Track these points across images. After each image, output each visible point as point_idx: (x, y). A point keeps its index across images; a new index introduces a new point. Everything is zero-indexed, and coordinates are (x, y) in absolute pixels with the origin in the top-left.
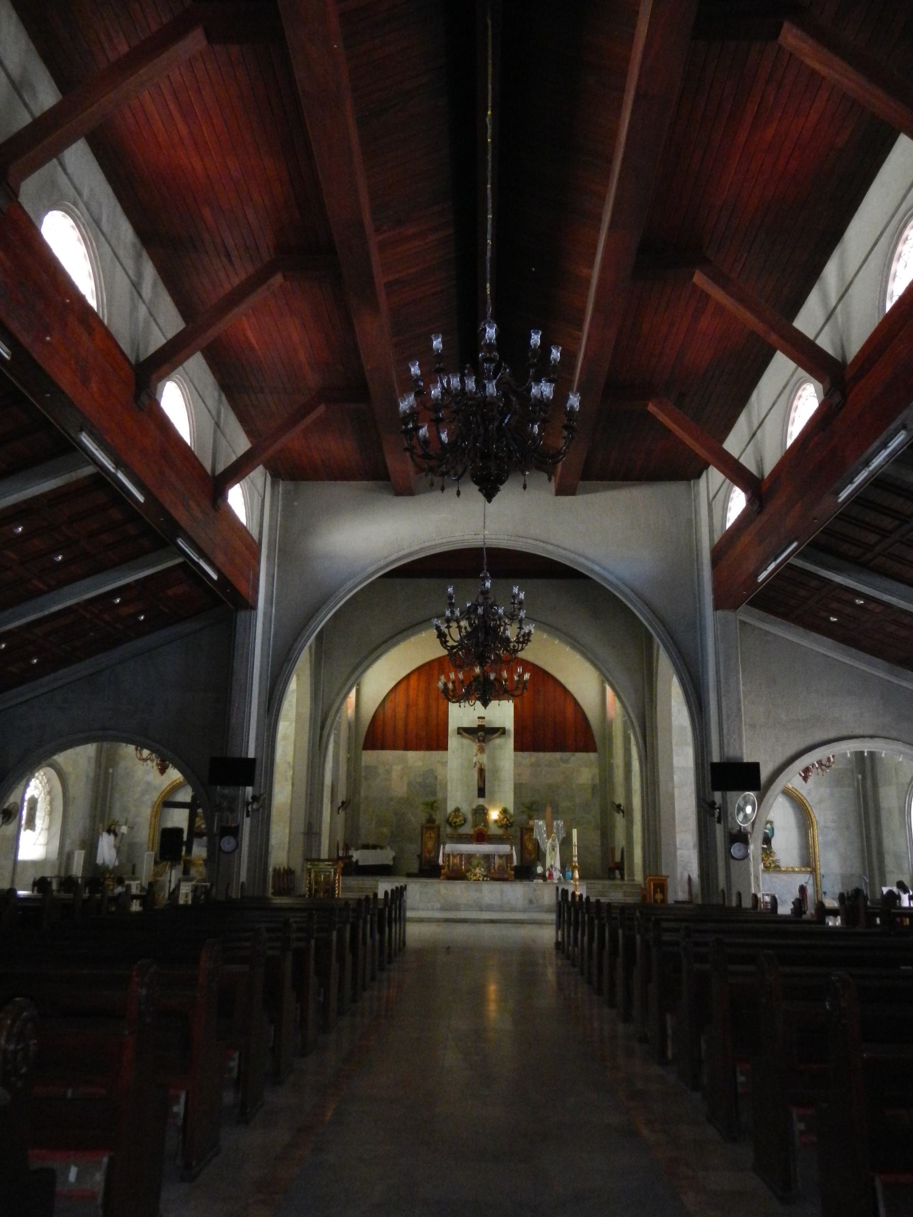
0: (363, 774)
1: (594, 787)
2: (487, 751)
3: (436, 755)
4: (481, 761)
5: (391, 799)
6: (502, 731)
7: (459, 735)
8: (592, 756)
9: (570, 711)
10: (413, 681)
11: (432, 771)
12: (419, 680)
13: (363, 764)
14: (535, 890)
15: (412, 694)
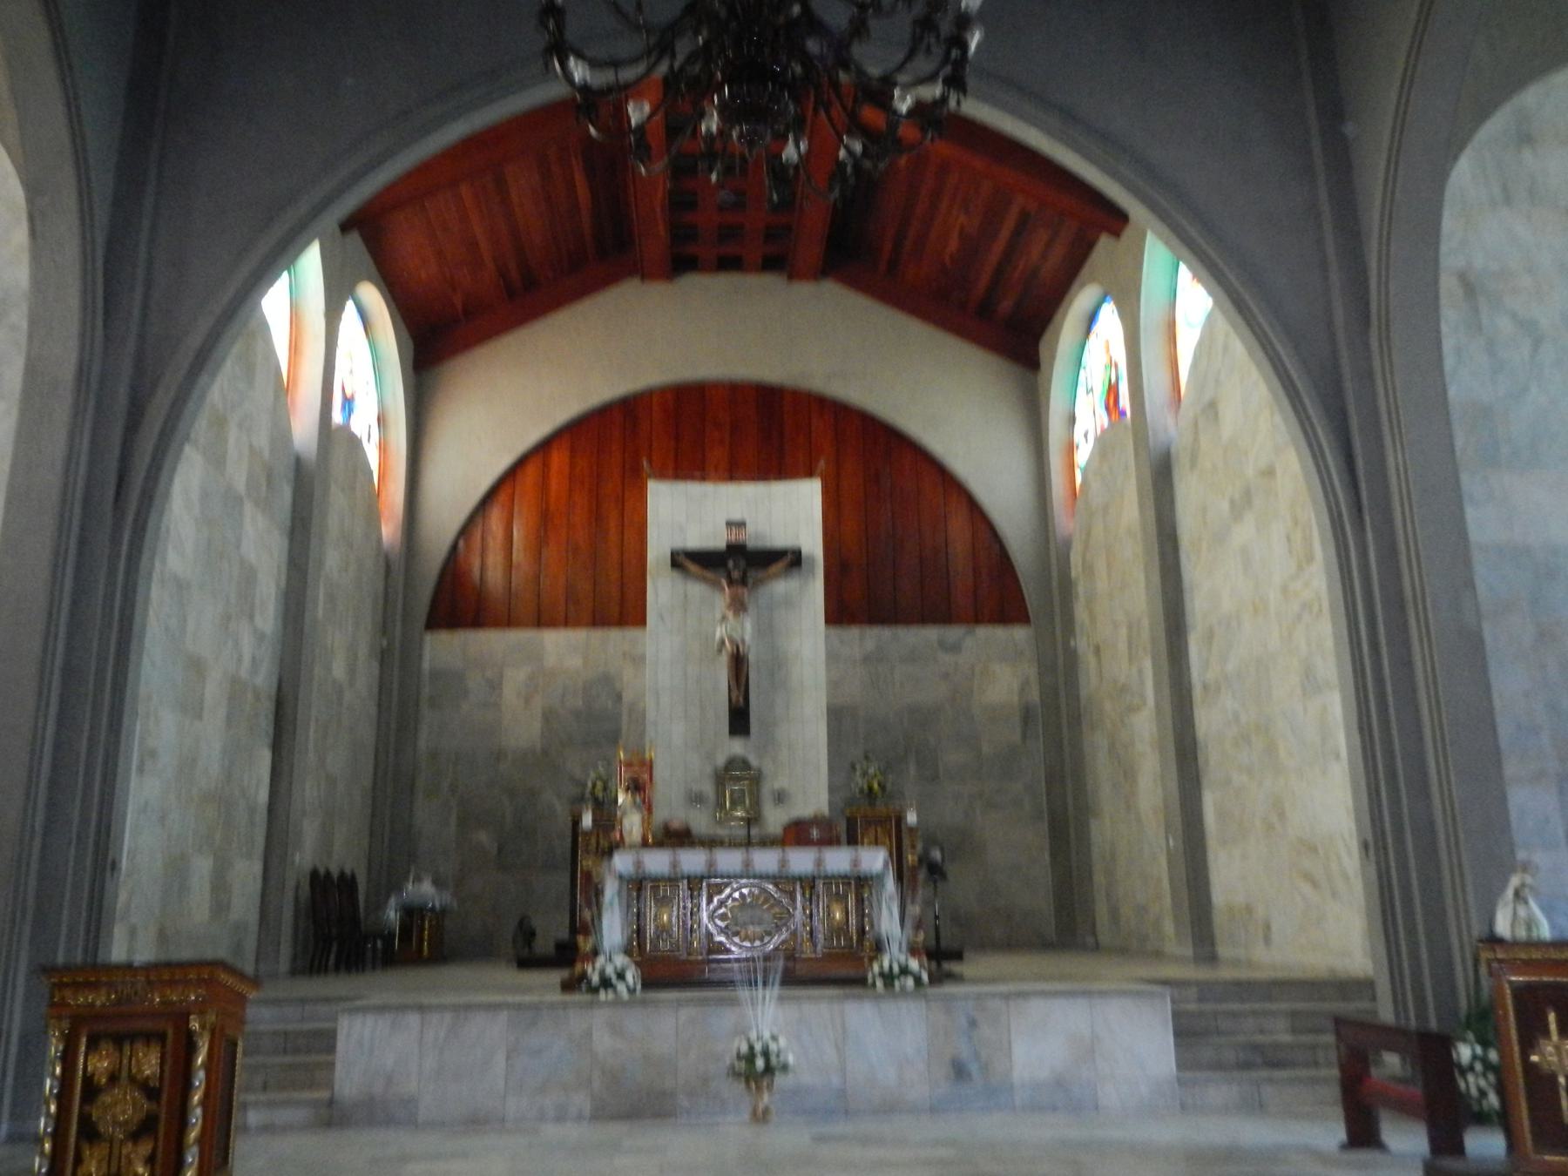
0: (426, 691)
1: (1027, 715)
2: (751, 608)
3: (616, 639)
4: (737, 637)
5: (499, 755)
6: (793, 559)
7: (676, 575)
8: (1019, 634)
9: (958, 527)
10: (559, 459)
11: (607, 680)
12: (573, 451)
13: (426, 665)
14: (973, 1023)
15: (556, 483)
